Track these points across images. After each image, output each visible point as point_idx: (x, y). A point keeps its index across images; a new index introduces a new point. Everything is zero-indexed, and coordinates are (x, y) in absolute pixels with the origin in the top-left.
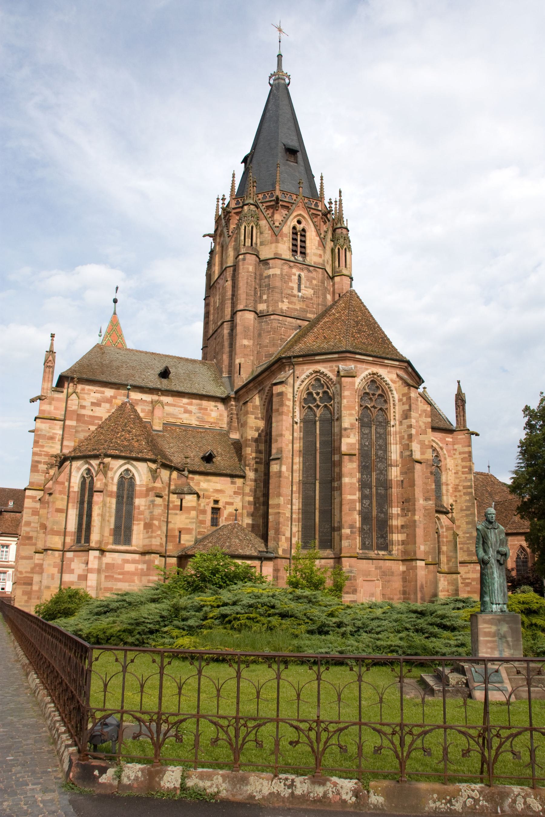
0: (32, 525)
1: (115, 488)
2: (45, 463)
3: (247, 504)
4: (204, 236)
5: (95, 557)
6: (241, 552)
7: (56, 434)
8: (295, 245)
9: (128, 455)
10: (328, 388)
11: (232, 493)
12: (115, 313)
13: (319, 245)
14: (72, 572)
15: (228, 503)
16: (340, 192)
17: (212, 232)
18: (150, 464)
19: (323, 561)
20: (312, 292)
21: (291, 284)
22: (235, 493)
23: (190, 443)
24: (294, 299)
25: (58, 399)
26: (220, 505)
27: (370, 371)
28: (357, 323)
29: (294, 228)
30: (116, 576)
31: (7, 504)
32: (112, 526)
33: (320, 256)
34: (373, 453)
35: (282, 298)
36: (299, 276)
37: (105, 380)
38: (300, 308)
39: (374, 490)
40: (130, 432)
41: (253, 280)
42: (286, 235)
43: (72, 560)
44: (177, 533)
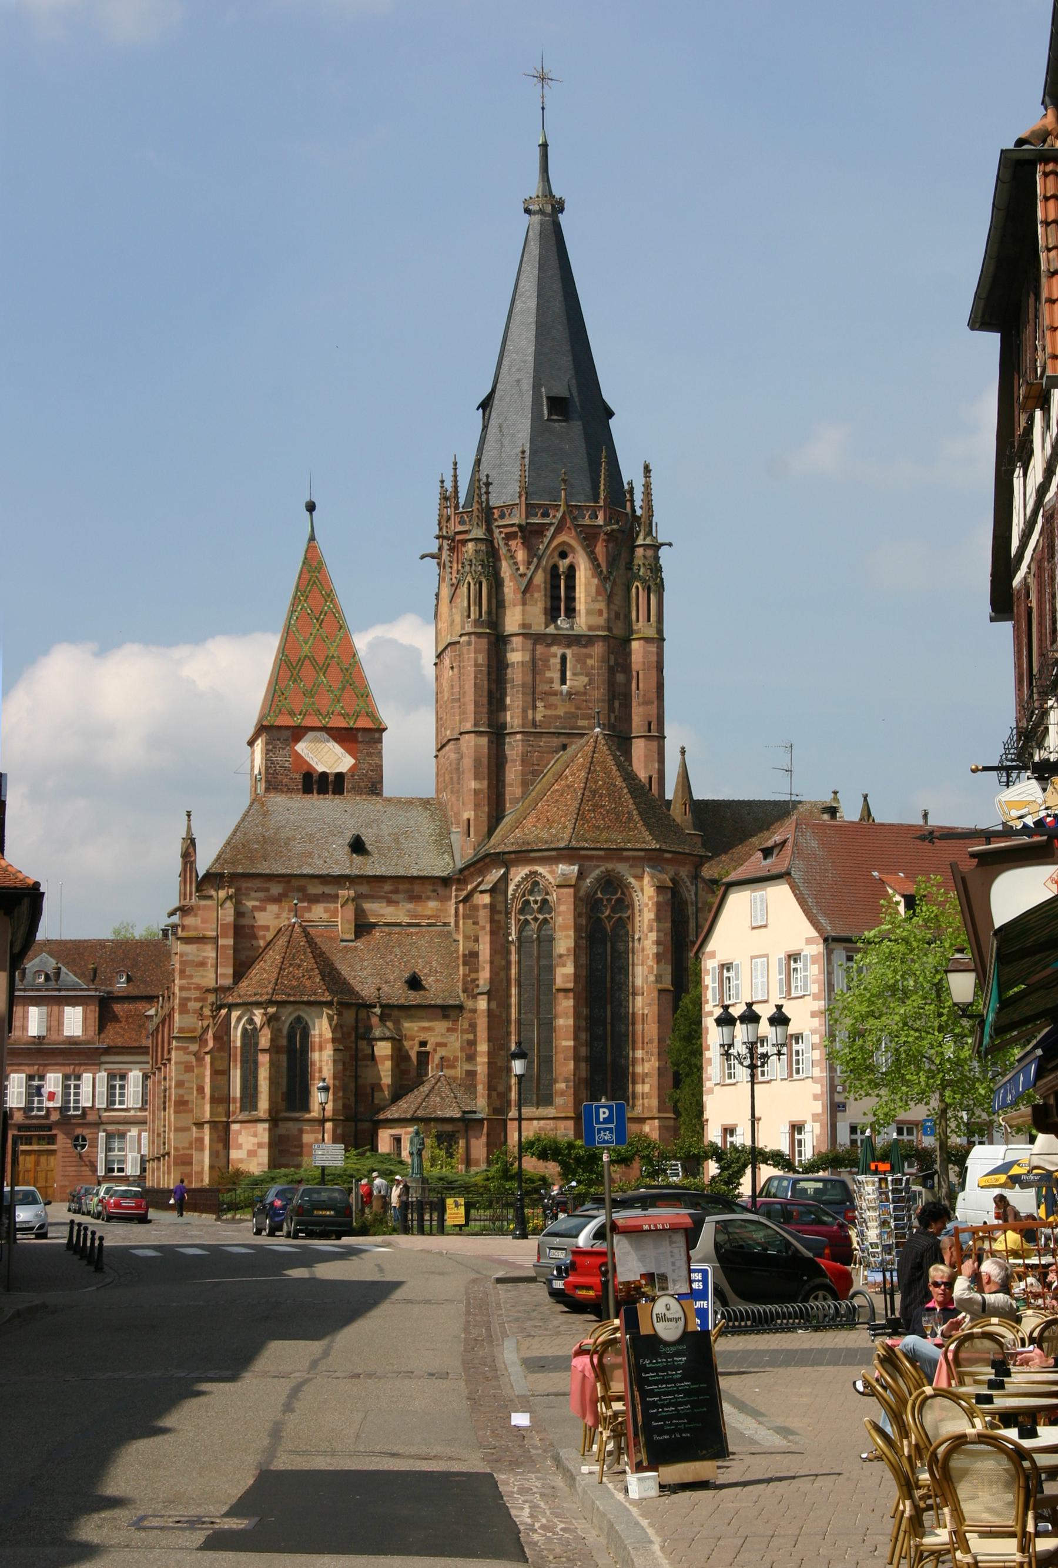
0: (187, 1085)
1: (284, 1042)
2: (197, 1000)
3: (465, 1044)
4: (423, 557)
5: (264, 1129)
6: (439, 1114)
7: (208, 958)
8: (555, 598)
9: (298, 999)
10: (547, 894)
11: (444, 1031)
12: (312, 538)
13: (598, 593)
14: (240, 1147)
15: (439, 1045)
16: (647, 470)
17: (435, 550)
18: (326, 1011)
19: (542, 1122)
20: (586, 680)
21: (548, 674)
22: (449, 1030)
23: (392, 957)
24: (553, 699)
25: (205, 908)
26: (428, 1048)
27: (602, 869)
28: (594, 792)
29: (555, 567)
30: (292, 1150)
31: (110, 981)
32: (284, 1089)
33: (600, 612)
34: (608, 979)
35: (534, 701)
36: (564, 658)
37: (268, 871)
38: (566, 713)
39: (609, 1027)
40: (299, 966)
41: (485, 678)
42: (539, 586)
43: (239, 1132)
44: (369, 1090)
